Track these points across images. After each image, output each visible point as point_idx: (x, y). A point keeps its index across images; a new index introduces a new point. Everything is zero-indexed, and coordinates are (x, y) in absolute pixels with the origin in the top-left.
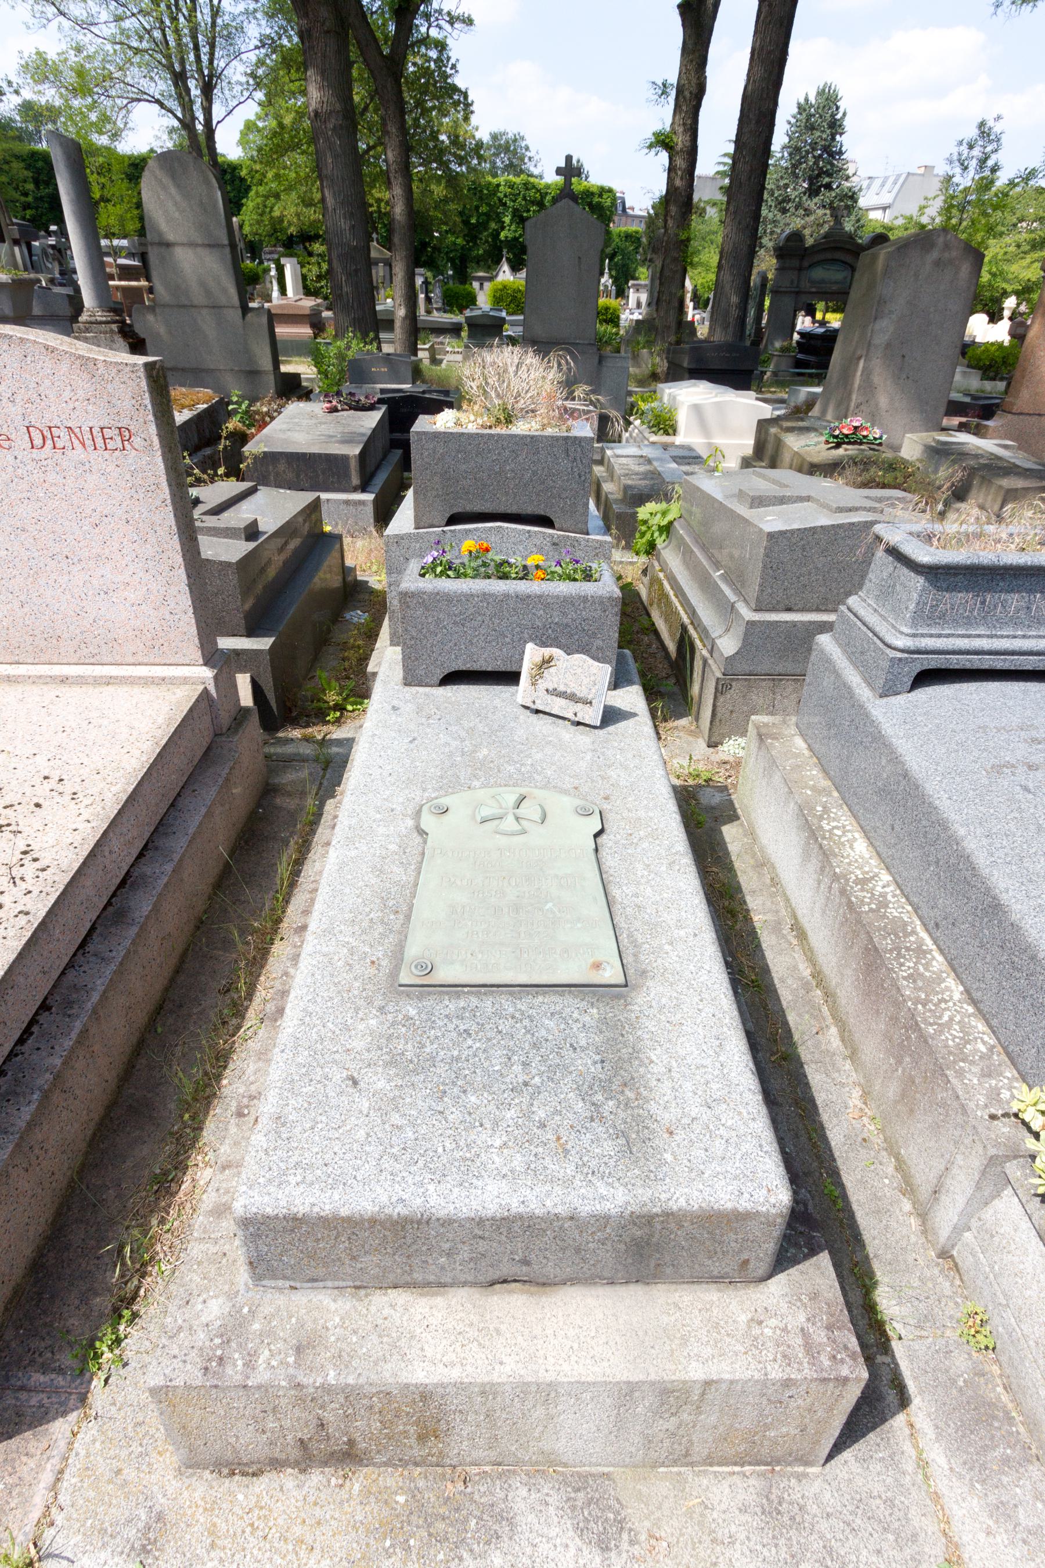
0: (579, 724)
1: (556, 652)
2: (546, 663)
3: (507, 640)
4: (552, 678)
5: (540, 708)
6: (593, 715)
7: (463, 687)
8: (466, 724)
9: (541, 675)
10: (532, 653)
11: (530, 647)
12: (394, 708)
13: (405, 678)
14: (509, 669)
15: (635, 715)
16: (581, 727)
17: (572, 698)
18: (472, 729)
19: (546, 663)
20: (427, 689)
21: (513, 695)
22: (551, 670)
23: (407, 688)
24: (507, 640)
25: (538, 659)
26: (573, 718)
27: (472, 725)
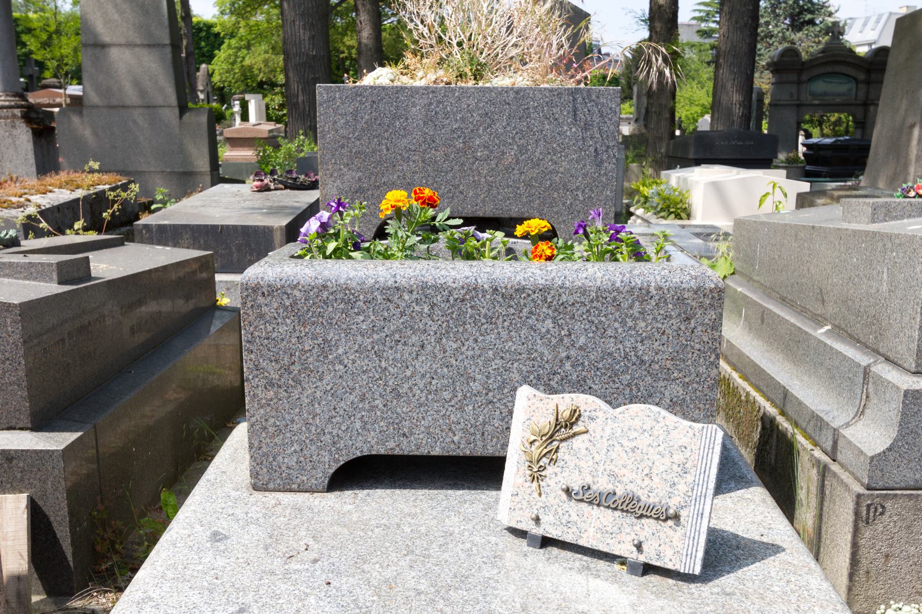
0: (648, 569)
1: (586, 402)
2: (565, 426)
3: (475, 386)
4: (577, 463)
5: (553, 533)
6: (682, 548)
7: (379, 492)
8: (376, 573)
9: (551, 455)
10: (531, 409)
11: (524, 393)
12: (216, 537)
13: (255, 474)
14: (479, 452)
15: (774, 549)
16: (654, 579)
17: (630, 506)
18: (390, 584)
19: (565, 426)
20: (301, 498)
21: (489, 507)
22: (577, 442)
23: (258, 495)
24: (475, 386)
25: (545, 421)
26: (631, 554)
27: (389, 573)
